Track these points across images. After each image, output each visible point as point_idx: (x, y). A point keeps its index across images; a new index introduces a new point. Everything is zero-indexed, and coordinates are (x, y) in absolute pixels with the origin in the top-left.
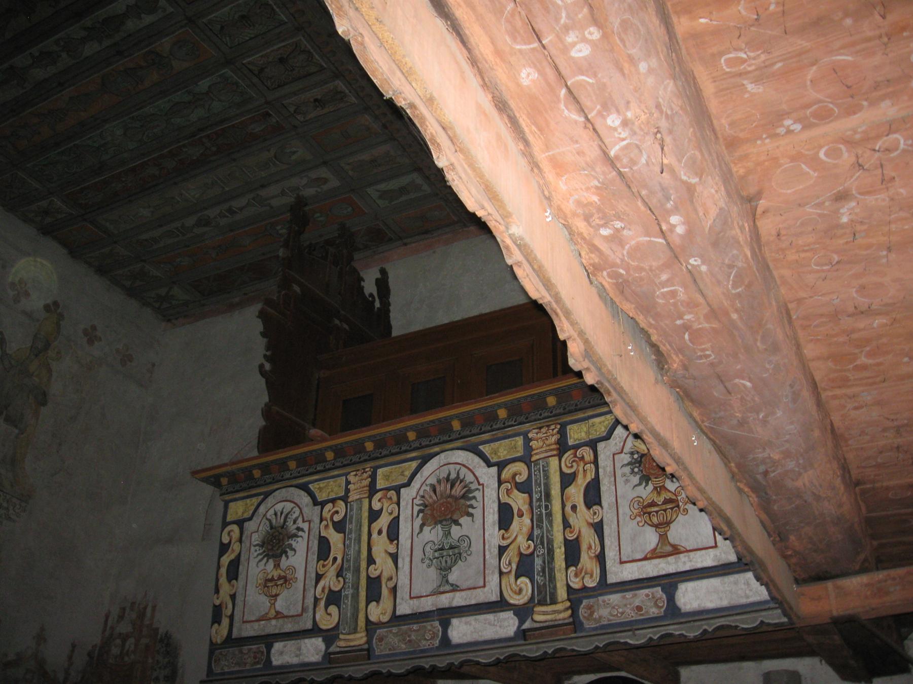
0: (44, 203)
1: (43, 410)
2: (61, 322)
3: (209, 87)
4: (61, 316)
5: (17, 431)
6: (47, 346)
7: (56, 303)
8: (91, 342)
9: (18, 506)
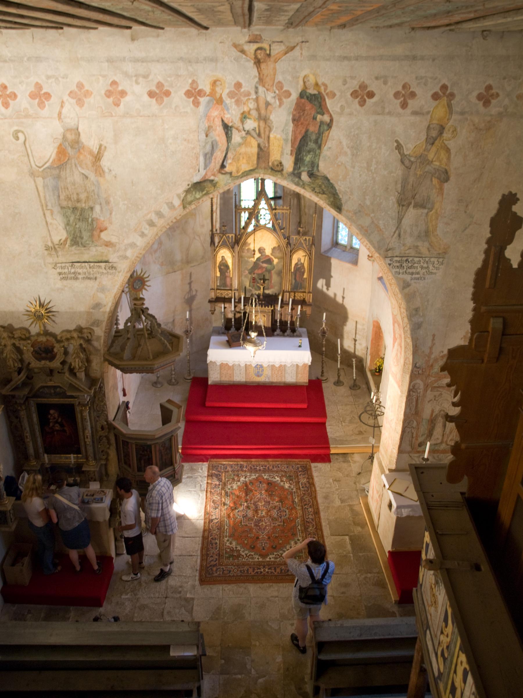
1: (446, 185)
2: (452, 102)
5: (426, 211)
6: (442, 129)
7: (444, 87)
8: (487, 103)
9: (436, 263)
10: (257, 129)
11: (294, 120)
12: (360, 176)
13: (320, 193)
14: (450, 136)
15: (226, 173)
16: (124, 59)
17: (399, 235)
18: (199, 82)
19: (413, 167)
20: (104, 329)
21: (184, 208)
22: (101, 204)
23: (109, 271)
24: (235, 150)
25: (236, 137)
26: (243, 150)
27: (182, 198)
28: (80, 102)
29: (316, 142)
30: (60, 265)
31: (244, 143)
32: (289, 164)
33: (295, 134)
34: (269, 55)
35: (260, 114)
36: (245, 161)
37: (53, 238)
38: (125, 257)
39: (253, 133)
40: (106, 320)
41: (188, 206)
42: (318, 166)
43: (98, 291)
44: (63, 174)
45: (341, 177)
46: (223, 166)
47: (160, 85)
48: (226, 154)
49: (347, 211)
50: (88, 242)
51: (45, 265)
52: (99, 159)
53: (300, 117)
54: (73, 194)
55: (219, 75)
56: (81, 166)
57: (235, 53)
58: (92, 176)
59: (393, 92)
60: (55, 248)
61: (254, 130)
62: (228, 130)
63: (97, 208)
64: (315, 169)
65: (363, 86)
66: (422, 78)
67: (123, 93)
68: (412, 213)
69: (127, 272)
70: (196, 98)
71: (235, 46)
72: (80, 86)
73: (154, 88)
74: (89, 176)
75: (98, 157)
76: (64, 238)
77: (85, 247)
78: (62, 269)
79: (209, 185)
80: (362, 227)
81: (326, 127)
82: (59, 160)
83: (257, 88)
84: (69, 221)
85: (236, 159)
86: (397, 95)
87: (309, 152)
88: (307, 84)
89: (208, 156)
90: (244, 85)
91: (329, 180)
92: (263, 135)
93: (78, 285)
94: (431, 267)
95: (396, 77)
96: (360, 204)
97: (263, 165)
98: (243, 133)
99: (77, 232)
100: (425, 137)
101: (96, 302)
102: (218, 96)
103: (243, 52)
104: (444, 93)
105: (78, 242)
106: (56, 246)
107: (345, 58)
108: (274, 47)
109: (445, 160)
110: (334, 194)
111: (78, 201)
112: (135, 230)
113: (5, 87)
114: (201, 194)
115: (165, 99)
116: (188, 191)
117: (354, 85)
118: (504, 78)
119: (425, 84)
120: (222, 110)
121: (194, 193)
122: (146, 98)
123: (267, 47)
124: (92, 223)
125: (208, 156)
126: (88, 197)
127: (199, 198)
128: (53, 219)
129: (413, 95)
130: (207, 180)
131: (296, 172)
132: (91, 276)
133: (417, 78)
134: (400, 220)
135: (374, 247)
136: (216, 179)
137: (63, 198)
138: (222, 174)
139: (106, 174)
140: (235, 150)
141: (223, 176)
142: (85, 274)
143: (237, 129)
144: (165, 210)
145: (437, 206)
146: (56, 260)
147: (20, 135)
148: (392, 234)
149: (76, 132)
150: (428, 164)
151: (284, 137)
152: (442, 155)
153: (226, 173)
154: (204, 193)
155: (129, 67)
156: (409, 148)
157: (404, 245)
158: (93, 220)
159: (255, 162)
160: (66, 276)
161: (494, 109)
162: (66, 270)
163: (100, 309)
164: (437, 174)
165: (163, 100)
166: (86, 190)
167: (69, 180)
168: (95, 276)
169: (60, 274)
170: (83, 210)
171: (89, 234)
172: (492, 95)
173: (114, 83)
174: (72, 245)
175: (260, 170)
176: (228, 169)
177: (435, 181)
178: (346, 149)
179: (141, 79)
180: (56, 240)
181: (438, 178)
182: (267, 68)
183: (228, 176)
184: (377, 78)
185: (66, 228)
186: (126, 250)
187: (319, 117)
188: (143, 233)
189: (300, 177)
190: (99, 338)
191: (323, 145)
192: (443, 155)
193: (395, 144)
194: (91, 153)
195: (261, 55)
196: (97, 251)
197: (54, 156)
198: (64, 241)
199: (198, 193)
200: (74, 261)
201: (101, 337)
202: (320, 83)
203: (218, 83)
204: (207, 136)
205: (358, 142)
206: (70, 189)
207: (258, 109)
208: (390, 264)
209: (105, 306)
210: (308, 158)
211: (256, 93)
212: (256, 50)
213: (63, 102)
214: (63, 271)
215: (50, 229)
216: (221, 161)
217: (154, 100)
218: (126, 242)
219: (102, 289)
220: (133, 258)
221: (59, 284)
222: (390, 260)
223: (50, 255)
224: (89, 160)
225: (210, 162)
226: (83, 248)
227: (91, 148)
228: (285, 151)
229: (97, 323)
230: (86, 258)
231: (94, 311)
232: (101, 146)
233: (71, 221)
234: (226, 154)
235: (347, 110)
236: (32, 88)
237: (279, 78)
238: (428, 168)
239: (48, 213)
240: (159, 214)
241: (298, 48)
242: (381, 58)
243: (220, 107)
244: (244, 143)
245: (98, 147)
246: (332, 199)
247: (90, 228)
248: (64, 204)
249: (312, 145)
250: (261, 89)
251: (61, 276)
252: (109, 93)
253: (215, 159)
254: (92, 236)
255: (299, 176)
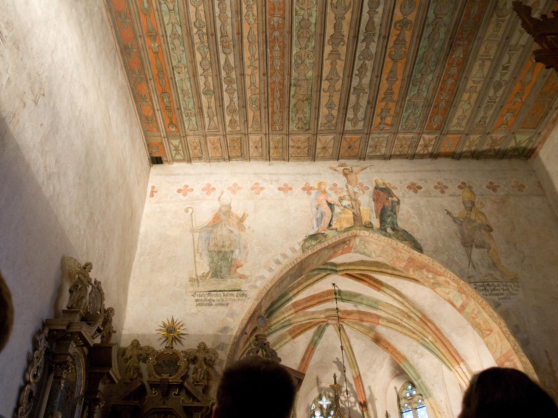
0: (421, 142)
3: (434, 13)
4: (470, 188)
5: (486, 250)
6: (473, 204)
8: (494, 190)
10: (351, 205)
11: (374, 200)
12: (429, 229)
13: (403, 240)
14: (480, 206)
15: (333, 229)
16: (264, 173)
17: (474, 266)
18: (310, 183)
19: (464, 224)
20: (228, 353)
21: (303, 251)
22: (240, 249)
23: (240, 297)
24: (337, 216)
25: (337, 210)
26: (343, 216)
27: (301, 245)
28: (234, 192)
29: (392, 211)
30: (198, 293)
31: (343, 212)
32: (376, 223)
33: (377, 207)
34: (352, 172)
35: (351, 198)
36: (345, 222)
37: (198, 272)
38: (255, 287)
39: (348, 207)
40: (231, 344)
41: (306, 250)
42: (397, 224)
43: (227, 316)
44: (215, 230)
45: (415, 231)
46: (330, 225)
47: (286, 185)
48: (332, 218)
49: (427, 251)
50: (225, 275)
51: (186, 293)
52: (243, 221)
53: (378, 199)
54: (220, 242)
55: (322, 180)
56: (229, 225)
57: (331, 171)
58: (236, 231)
59: (433, 186)
60: (197, 279)
61: (349, 205)
62: (331, 206)
63: (237, 252)
64: (395, 226)
65: (413, 184)
66: (447, 179)
67: (262, 188)
68: (476, 253)
69: (256, 299)
70: (309, 190)
71: (331, 168)
72: (235, 185)
73: (282, 186)
74: (234, 231)
75: (241, 220)
76: (206, 272)
77: (222, 278)
78: (199, 296)
79: (322, 236)
80: (443, 262)
81: (396, 204)
82: (214, 222)
83: (347, 186)
84: (213, 260)
85: (339, 221)
86: (436, 187)
87: (389, 216)
88: (378, 183)
89: (319, 220)
90: (338, 184)
91: (407, 232)
92: (355, 208)
93: (210, 310)
94: (510, 289)
95: (431, 179)
96: (435, 247)
97: (359, 224)
98: (342, 208)
99: (218, 267)
100: (464, 207)
101: (225, 325)
102: (323, 190)
103: (336, 170)
104: (465, 186)
105: (218, 275)
106: (199, 278)
107: (398, 172)
108: (353, 168)
109: (483, 219)
110: (414, 241)
111: (223, 246)
112: (265, 267)
113: (188, 186)
114: (315, 242)
115: (289, 191)
116: (305, 240)
117: (408, 183)
118: (498, 179)
119: (451, 182)
120: (326, 196)
121: (310, 241)
122: (277, 191)
123: (350, 168)
124: (231, 262)
125: (319, 220)
126: (231, 244)
127: (315, 245)
128: (201, 259)
129: (446, 187)
130: (320, 233)
131: (382, 228)
132: (224, 302)
133: (444, 179)
134: (469, 256)
135: (457, 276)
136: (326, 233)
137: (212, 245)
138: (330, 230)
139: (246, 230)
140: (337, 216)
141: (331, 231)
142: (219, 301)
143: (337, 205)
144: (289, 253)
145: (492, 246)
146: (196, 289)
147: (190, 211)
148: (468, 266)
149: (230, 207)
150: (473, 222)
151: (369, 208)
152: (480, 217)
153: (333, 229)
154: (318, 241)
155: (267, 177)
156: (456, 214)
157: (480, 273)
158: (232, 260)
159: (353, 222)
160: (202, 302)
161: (501, 192)
162: (203, 298)
163: (228, 332)
164: (482, 227)
165: (288, 192)
166: (230, 239)
167: (218, 234)
168: (227, 302)
169: (197, 300)
170: (225, 253)
171: (227, 269)
172: (495, 186)
173: (257, 184)
174: (212, 277)
175: (357, 227)
176: (333, 227)
177: (483, 232)
178: (413, 215)
179: (274, 182)
180: (200, 273)
181: (485, 230)
182: (352, 177)
183: (334, 231)
184: (420, 180)
185: (210, 265)
186: (256, 281)
187: (390, 198)
188: (271, 269)
189: (386, 232)
190: (222, 361)
191: (397, 213)
192: (480, 217)
193: (446, 212)
194: (237, 217)
195: (346, 171)
196: (232, 282)
197: (210, 220)
198: (207, 274)
199: (313, 241)
200: (211, 290)
201: (224, 361)
202: (386, 183)
203: (322, 184)
204: (317, 209)
205: (420, 211)
206: (218, 239)
207: (349, 195)
208: (476, 288)
209: (232, 330)
210: (389, 220)
211: (347, 188)
212: (343, 170)
213: (223, 192)
214: (200, 298)
215: (197, 265)
216: (328, 223)
217: (282, 192)
218: (256, 274)
219: (232, 314)
220: (262, 287)
221: (194, 310)
222: (474, 285)
223: (192, 285)
224: (235, 221)
225: (321, 223)
226: (220, 280)
227: (238, 215)
228: (372, 216)
229: (222, 346)
230: (222, 287)
231: (221, 334)
232: (244, 214)
233: (215, 261)
234: (332, 218)
235: (407, 195)
236: (205, 186)
237: (360, 181)
238: (474, 224)
239: (198, 256)
240: (284, 256)
241: (368, 168)
242: (419, 171)
243: (325, 195)
244: (343, 212)
245: (242, 214)
246: (413, 244)
247: (229, 265)
248: (212, 249)
249: (389, 213)
250: (349, 186)
251: (198, 303)
252: (253, 189)
253: (324, 221)
254: (230, 270)
255: (385, 230)
